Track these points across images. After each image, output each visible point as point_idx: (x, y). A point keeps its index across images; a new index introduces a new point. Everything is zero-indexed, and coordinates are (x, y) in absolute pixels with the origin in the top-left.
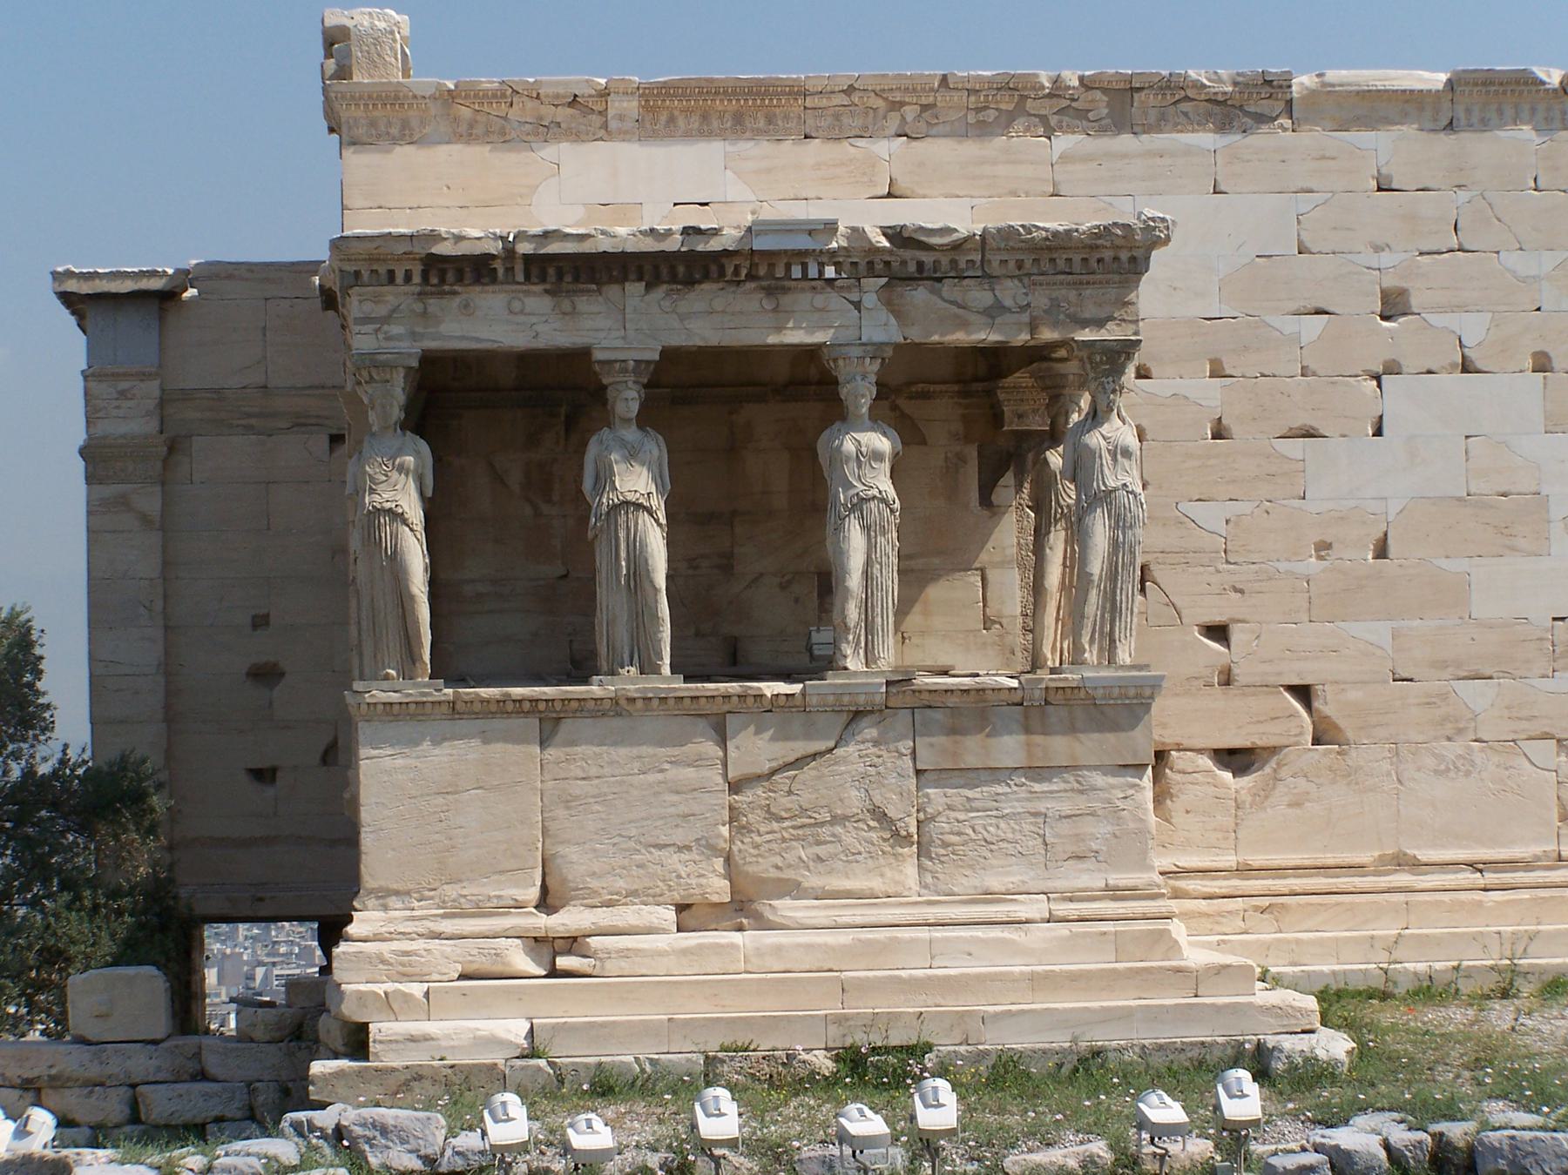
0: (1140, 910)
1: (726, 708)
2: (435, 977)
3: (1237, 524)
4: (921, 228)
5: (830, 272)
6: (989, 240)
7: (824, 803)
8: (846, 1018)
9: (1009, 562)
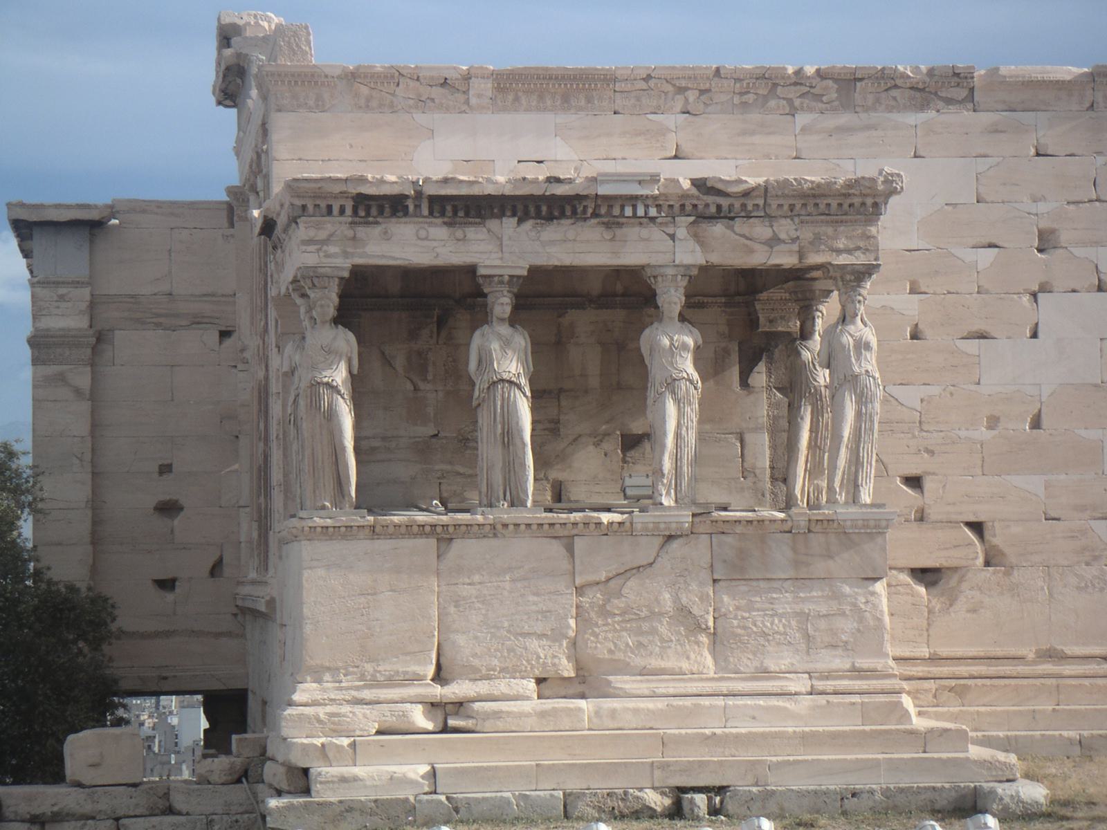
0: (879, 687)
1: (575, 532)
2: (358, 733)
3: (929, 402)
4: (721, 180)
5: (653, 212)
6: (772, 192)
8: (668, 764)
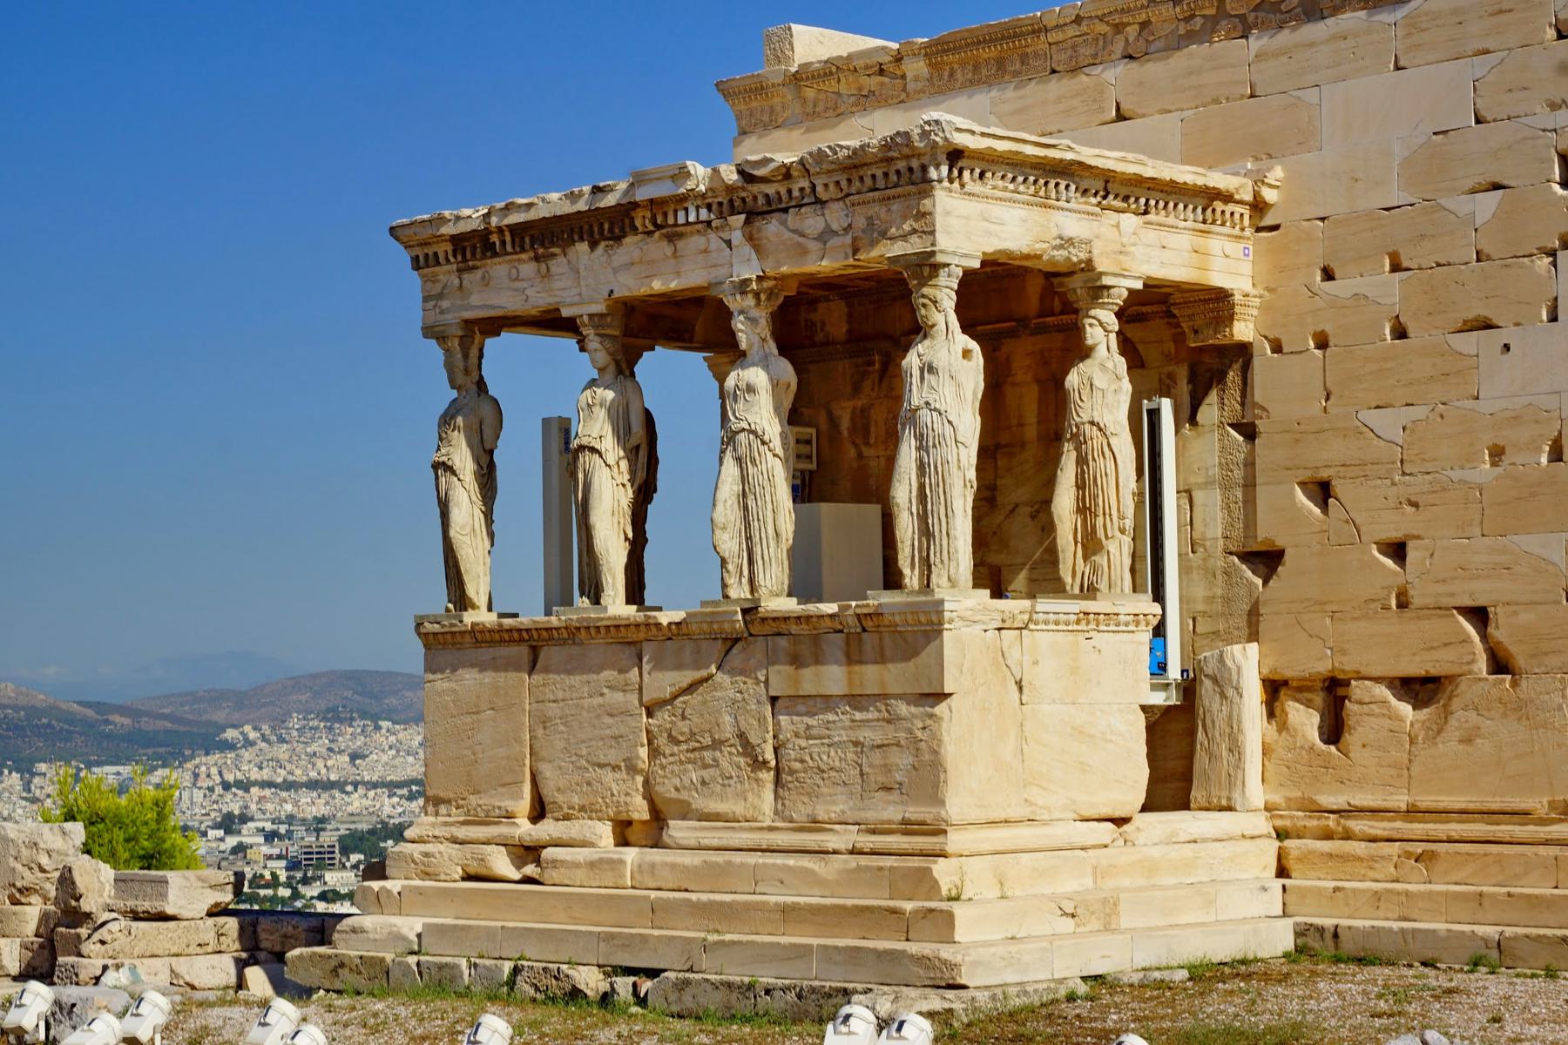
1: (642, 636)
3: (1413, 431)
7: (708, 727)
9: (1213, 483)
